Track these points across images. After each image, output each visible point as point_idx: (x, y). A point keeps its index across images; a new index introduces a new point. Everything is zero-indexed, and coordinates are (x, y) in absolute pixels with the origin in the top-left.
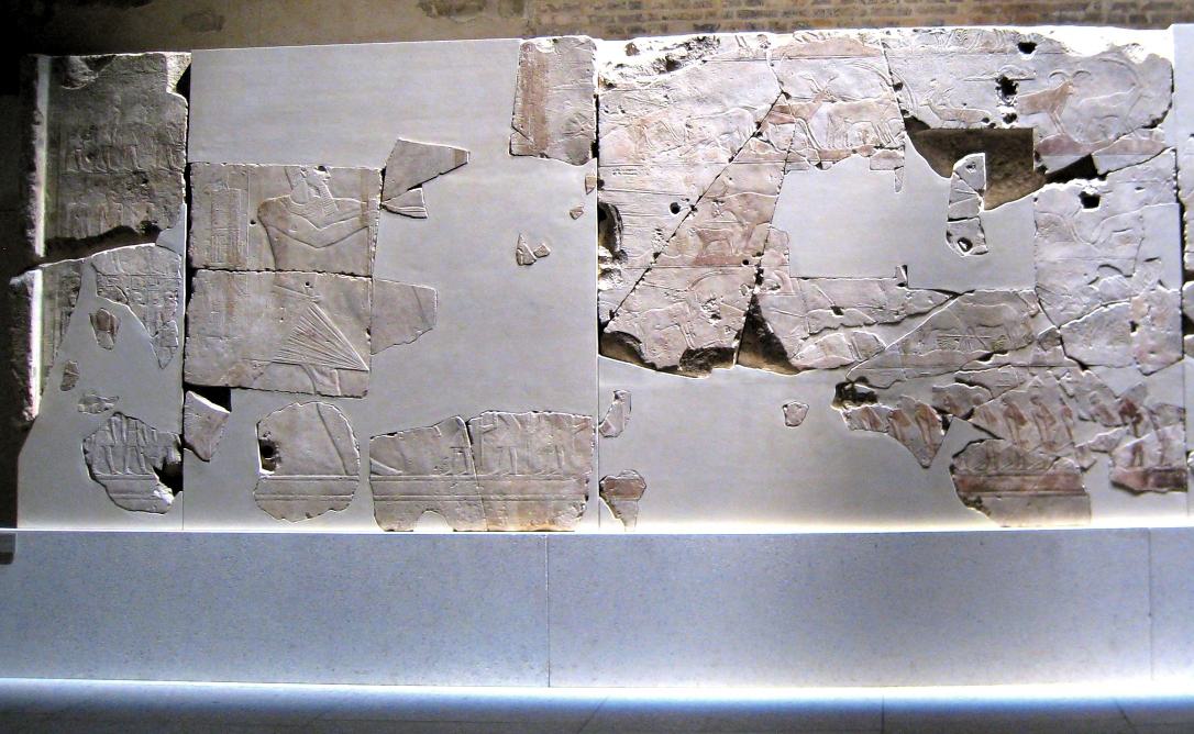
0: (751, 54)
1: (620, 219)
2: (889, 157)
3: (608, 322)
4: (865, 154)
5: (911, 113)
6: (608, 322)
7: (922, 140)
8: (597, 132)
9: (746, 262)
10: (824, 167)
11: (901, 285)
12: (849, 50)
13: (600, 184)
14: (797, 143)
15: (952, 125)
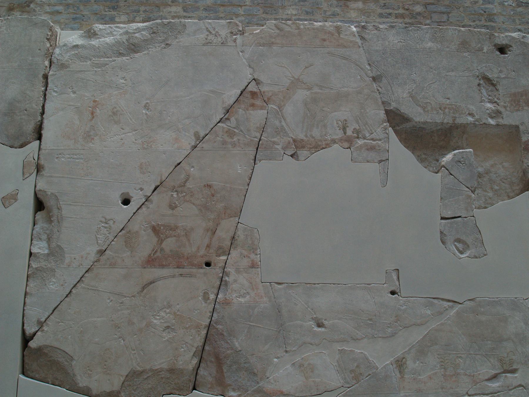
0: (220, 39)
1: (59, 209)
2: (372, 148)
3: (35, 334)
4: (346, 145)
5: (393, 105)
6: (35, 334)
8: (43, 113)
9: (208, 264)
10: (301, 158)
11: (393, 293)
12: (324, 40)
13: (39, 168)
15: (439, 118)
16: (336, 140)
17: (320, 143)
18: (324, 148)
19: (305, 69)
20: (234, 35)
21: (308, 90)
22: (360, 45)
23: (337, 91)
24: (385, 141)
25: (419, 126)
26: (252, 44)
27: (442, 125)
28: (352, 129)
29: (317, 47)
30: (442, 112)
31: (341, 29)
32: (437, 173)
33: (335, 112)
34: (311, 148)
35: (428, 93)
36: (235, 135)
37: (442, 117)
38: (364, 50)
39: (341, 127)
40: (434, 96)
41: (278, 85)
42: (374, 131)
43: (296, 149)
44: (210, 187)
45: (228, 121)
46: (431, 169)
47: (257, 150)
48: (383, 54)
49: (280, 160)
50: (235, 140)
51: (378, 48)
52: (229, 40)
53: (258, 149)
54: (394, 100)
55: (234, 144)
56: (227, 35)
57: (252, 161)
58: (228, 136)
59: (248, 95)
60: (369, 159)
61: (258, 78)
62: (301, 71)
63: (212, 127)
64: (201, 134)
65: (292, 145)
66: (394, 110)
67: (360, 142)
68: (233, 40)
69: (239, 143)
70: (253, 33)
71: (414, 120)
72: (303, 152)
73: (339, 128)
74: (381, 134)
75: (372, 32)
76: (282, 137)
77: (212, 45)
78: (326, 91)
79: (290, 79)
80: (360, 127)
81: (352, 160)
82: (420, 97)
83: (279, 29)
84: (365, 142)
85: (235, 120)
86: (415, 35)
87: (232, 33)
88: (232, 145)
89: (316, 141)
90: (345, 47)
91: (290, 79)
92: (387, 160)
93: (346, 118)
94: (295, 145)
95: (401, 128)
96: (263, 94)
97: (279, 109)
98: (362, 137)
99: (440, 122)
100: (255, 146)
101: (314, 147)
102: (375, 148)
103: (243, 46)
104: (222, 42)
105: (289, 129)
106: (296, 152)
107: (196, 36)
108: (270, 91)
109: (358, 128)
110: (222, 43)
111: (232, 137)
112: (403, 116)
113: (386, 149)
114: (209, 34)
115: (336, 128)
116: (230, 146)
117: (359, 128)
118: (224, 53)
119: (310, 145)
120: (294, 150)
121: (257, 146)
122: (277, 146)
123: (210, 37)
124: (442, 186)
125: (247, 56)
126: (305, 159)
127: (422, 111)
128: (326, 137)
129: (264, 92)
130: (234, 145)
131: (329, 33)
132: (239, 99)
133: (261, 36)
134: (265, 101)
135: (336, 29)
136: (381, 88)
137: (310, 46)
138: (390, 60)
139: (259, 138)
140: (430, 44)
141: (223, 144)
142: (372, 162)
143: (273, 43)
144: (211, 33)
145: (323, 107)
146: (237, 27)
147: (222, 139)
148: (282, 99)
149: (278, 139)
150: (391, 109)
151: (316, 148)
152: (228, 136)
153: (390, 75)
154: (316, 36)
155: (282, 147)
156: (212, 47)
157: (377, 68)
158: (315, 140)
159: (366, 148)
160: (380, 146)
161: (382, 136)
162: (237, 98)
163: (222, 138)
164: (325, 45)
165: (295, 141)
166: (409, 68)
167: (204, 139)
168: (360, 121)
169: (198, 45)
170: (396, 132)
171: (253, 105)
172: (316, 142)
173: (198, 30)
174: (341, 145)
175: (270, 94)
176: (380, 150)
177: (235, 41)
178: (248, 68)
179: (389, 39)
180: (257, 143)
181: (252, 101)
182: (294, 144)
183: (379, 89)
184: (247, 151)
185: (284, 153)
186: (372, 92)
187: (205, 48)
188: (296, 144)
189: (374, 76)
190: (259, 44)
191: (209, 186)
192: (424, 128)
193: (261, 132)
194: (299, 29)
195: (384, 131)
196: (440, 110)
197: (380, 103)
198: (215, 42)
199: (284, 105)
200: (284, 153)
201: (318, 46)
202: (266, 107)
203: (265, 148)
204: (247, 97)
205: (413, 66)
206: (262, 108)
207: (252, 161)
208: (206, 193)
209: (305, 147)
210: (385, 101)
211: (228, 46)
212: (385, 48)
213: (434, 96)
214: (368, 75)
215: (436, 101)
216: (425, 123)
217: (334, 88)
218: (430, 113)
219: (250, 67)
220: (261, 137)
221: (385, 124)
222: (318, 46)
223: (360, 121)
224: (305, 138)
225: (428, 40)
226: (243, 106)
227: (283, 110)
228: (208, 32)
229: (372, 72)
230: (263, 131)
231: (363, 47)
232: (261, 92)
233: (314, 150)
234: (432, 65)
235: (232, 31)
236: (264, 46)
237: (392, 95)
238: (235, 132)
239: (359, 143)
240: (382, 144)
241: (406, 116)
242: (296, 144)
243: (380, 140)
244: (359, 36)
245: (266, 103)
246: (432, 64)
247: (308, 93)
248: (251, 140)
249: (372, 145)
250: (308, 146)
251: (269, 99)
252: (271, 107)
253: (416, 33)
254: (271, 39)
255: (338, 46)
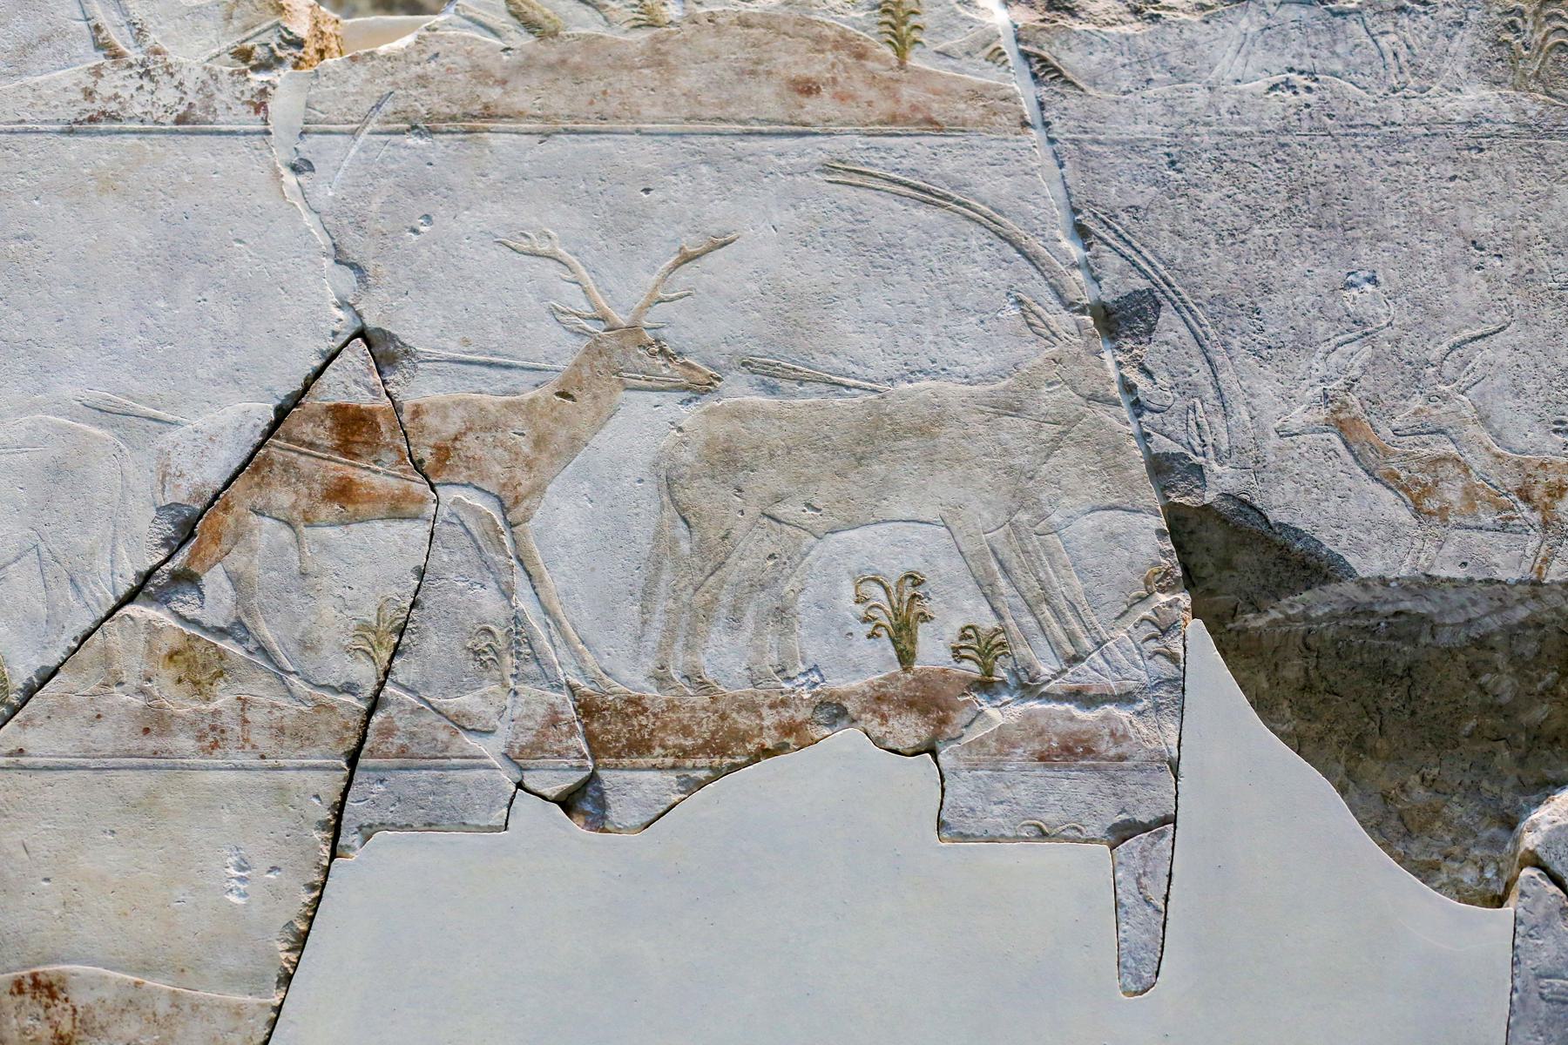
0: (168, 95)
4: (909, 730)
5: (1223, 479)
7: (1292, 671)
10: (618, 811)
12: (807, 88)
14: (433, 642)
16: (846, 704)
17: (743, 721)
18: (766, 753)
19: (677, 266)
20: (255, 69)
21: (687, 395)
22: (1029, 111)
23: (873, 396)
24: (1157, 708)
25: (1389, 608)
26: (365, 120)
27: (1535, 596)
28: (951, 634)
29: (761, 134)
30: (1536, 517)
31: (913, 20)
32: (1499, 901)
33: (852, 525)
34: (686, 753)
35: (1445, 398)
36: (221, 674)
37: (1532, 544)
38: (1052, 141)
39: (887, 623)
40: (1485, 420)
41: (508, 367)
42: (1087, 643)
43: (594, 758)
44: (53, 996)
45: (186, 587)
46: (1469, 875)
47: (353, 759)
48: (1173, 163)
49: (492, 829)
50: (218, 704)
51: (1139, 130)
52: (223, 97)
53: (362, 762)
54: (1224, 447)
55: (213, 728)
56: (217, 68)
57: (320, 837)
58: (180, 681)
59: (320, 430)
60: (1048, 817)
61: (388, 329)
62: (655, 277)
63: (88, 624)
64: (20, 668)
65: (572, 732)
66: (1229, 506)
67: (1002, 713)
68: (247, 97)
69: (246, 721)
70: (371, 55)
71: (1350, 572)
72: (637, 774)
73: (869, 628)
74: (1134, 663)
75: (1112, 30)
76: (511, 682)
77: (119, 132)
78: (798, 402)
79: (581, 333)
80: (1000, 617)
81: (941, 825)
82: (1395, 424)
83: (530, 26)
84: (1029, 716)
85: (227, 585)
86: (1383, 41)
87: (244, 55)
88: (200, 738)
89: (721, 706)
90: (933, 125)
91: (581, 333)
92: (1164, 821)
93: (915, 564)
94: (590, 738)
95: (1275, 622)
96: (408, 426)
97: (505, 510)
98: (1012, 681)
99: (1519, 582)
100: (342, 740)
101: (707, 743)
102: (1088, 751)
103: (304, 132)
104: (182, 109)
105: (557, 639)
106: (593, 778)
107: (27, 80)
108: (458, 404)
109: (988, 622)
110: (181, 120)
111: (199, 690)
112: (1285, 548)
113: (1161, 753)
114: (108, 63)
115: (850, 629)
116: (184, 742)
117: (995, 624)
118: (187, 179)
119: (686, 731)
120: (580, 768)
121: (355, 741)
122: (473, 743)
123: (115, 82)
124: (1518, 982)
125: (326, 192)
126: (646, 819)
127: (1405, 515)
128: (787, 686)
129: (417, 412)
130: (212, 736)
131: (837, 46)
132: (265, 457)
133: (418, 70)
134: (418, 465)
135: (888, 18)
136: (1149, 374)
137: (720, 127)
138: (1211, 198)
139: (369, 691)
140: (1475, 97)
141: (146, 731)
142: (1067, 839)
143: (488, 114)
144: (116, 56)
145: (778, 499)
146: (278, 19)
147: (139, 702)
148: (526, 449)
149: (484, 696)
150: (1207, 507)
151: (722, 751)
152: (180, 681)
153: (1208, 292)
154: (758, 62)
155: (510, 747)
156: (117, 139)
157: (1128, 251)
158: (714, 700)
159: (1037, 746)
160: (1125, 736)
161: (1139, 673)
162: (250, 449)
163: (142, 692)
164: (808, 119)
165: (587, 709)
166: (1333, 245)
167: (33, 701)
168: (1002, 583)
169: (38, 132)
170: (1236, 648)
171: (342, 492)
172: (723, 717)
173: (46, 39)
174: (877, 730)
175: (453, 425)
176: (1121, 758)
177: (259, 104)
178: (328, 263)
179: (1211, 68)
180: (355, 722)
181: (339, 468)
182: (585, 726)
183: (1134, 376)
184: (287, 776)
185: (520, 785)
186: (1093, 398)
187: (75, 147)
188: (595, 726)
189: (1108, 297)
190: (406, 119)
191: (46, 989)
192: (1423, 618)
193: (386, 655)
194: (652, 25)
195: (1153, 645)
196: (1520, 505)
197: (1140, 470)
198: (138, 110)
199: (539, 489)
200: (520, 785)
201: (770, 122)
202: (422, 500)
203: (403, 752)
204: (311, 445)
205: (1358, 233)
206: (398, 509)
207: (317, 836)
208: (24, 1032)
209: (649, 748)
210: (1168, 457)
211: (219, 133)
212: (1188, 130)
213: (1485, 420)
214: (1071, 296)
215: (1499, 450)
216: (1426, 584)
217: (851, 382)
218: (1459, 526)
219: (340, 258)
220: (382, 685)
221: (1163, 598)
222: (770, 122)
223: (1002, 583)
224: (651, 692)
225: (1460, 69)
226: (283, 498)
227: (526, 519)
228: (100, 54)
229: (1097, 279)
230: (396, 651)
231: (1047, 124)
232: (398, 409)
233: (704, 761)
234: (1482, 223)
235: (249, 44)
236: (432, 132)
237: (1217, 420)
238: (222, 655)
239: (991, 720)
240: (1134, 719)
241: (1299, 546)
242: (595, 726)
243: (1127, 698)
244: (1026, 56)
245: (426, 477)
246: (1480, 220)
247: (690, 415)
248: (321, 707)
249: (1075, 727)
250: (671, 740)
251: (443, 453)
252: (457, 502)
253: (1391, 28)
254: (479, 89)
255: (893, 120)
